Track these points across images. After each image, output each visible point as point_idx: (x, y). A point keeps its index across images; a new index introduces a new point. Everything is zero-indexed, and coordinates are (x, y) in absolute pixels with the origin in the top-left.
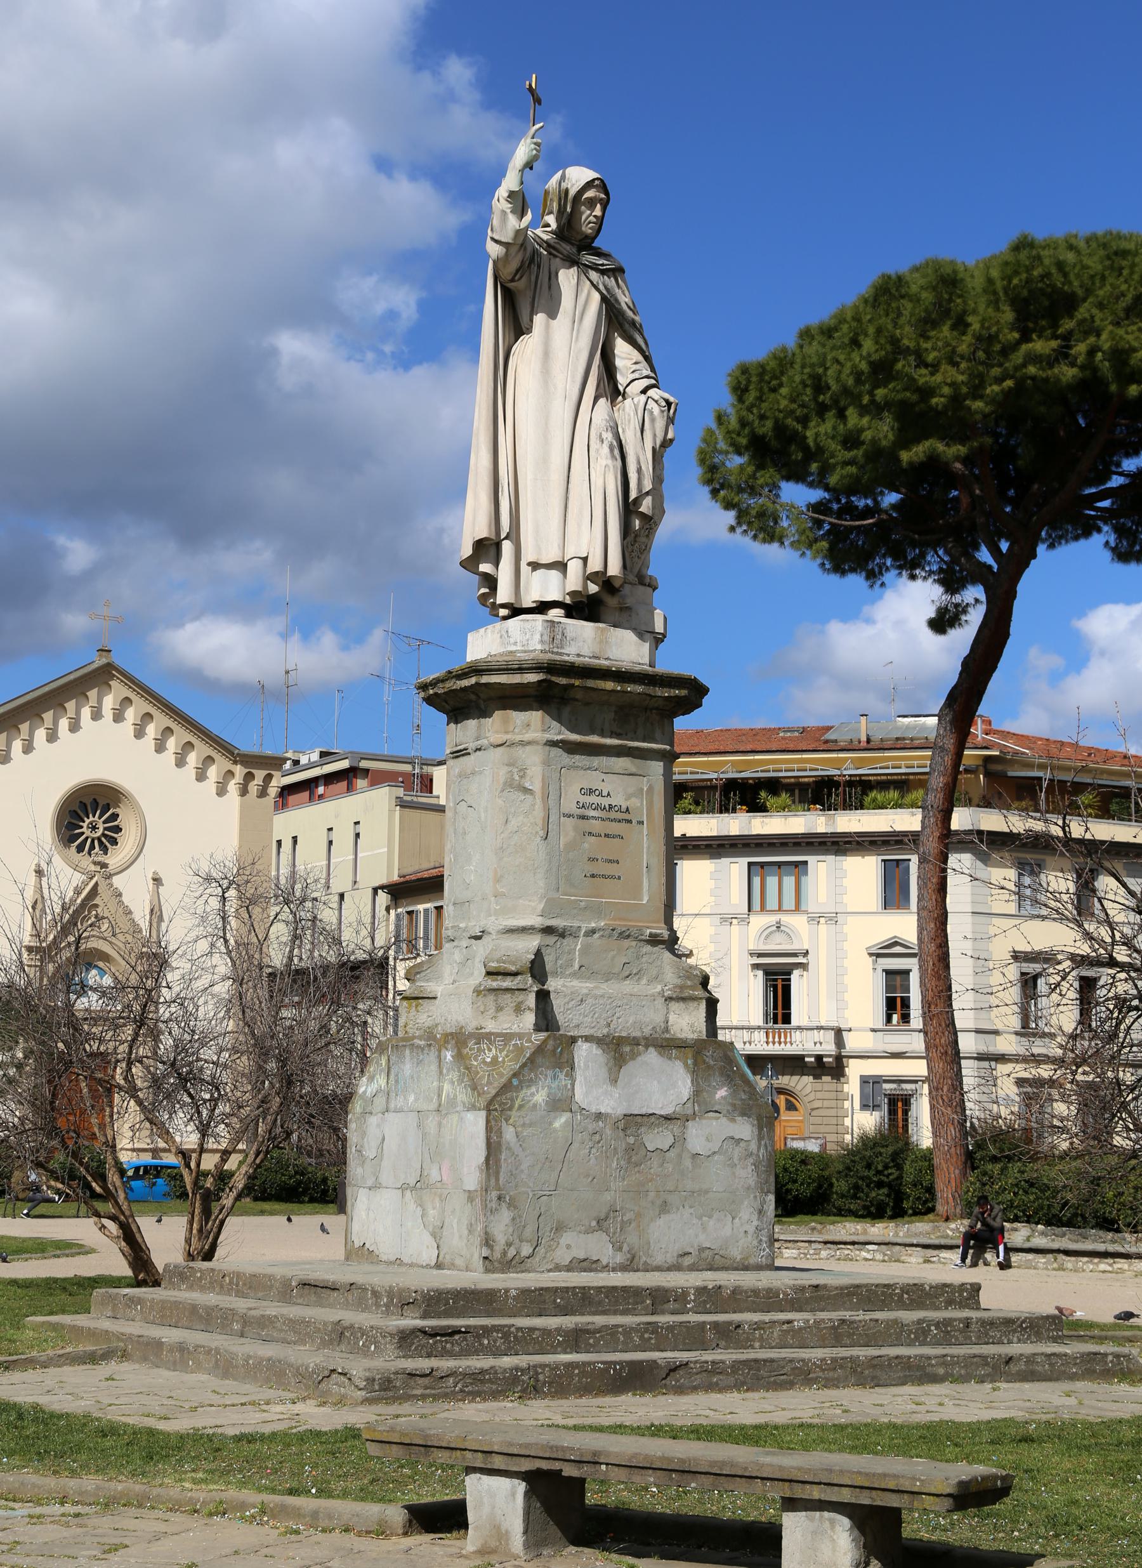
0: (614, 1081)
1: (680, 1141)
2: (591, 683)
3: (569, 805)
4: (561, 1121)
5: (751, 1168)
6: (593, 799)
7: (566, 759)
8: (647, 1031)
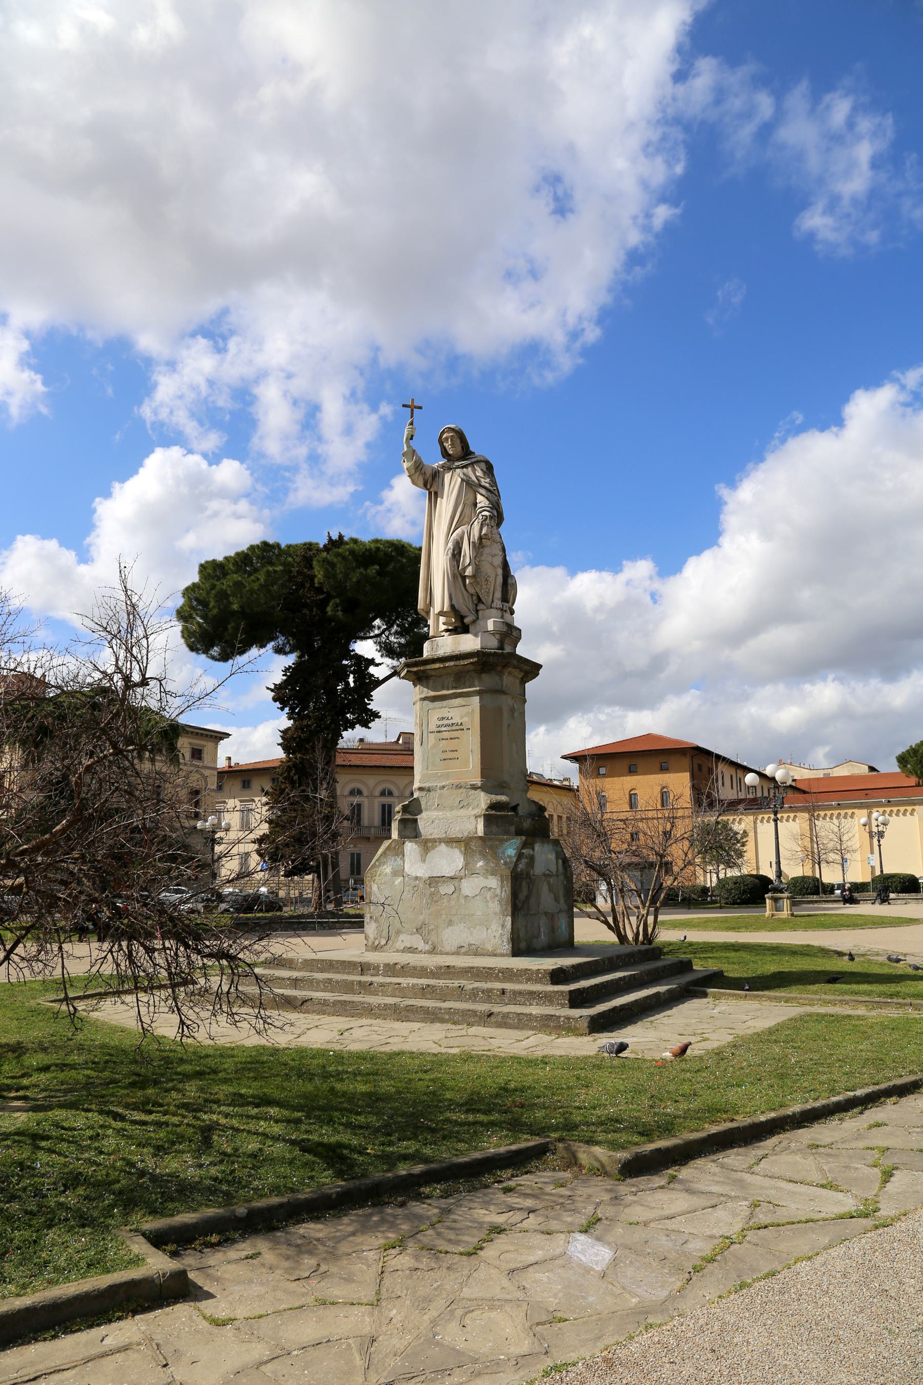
0: (424, 861)
1: (457, 890)
2: (428, 667)
3: (432, 727)
4: (399, 880)
5: (497, 903)
6: (445, 722)
7: (431, 705)
8: (466, 834)
